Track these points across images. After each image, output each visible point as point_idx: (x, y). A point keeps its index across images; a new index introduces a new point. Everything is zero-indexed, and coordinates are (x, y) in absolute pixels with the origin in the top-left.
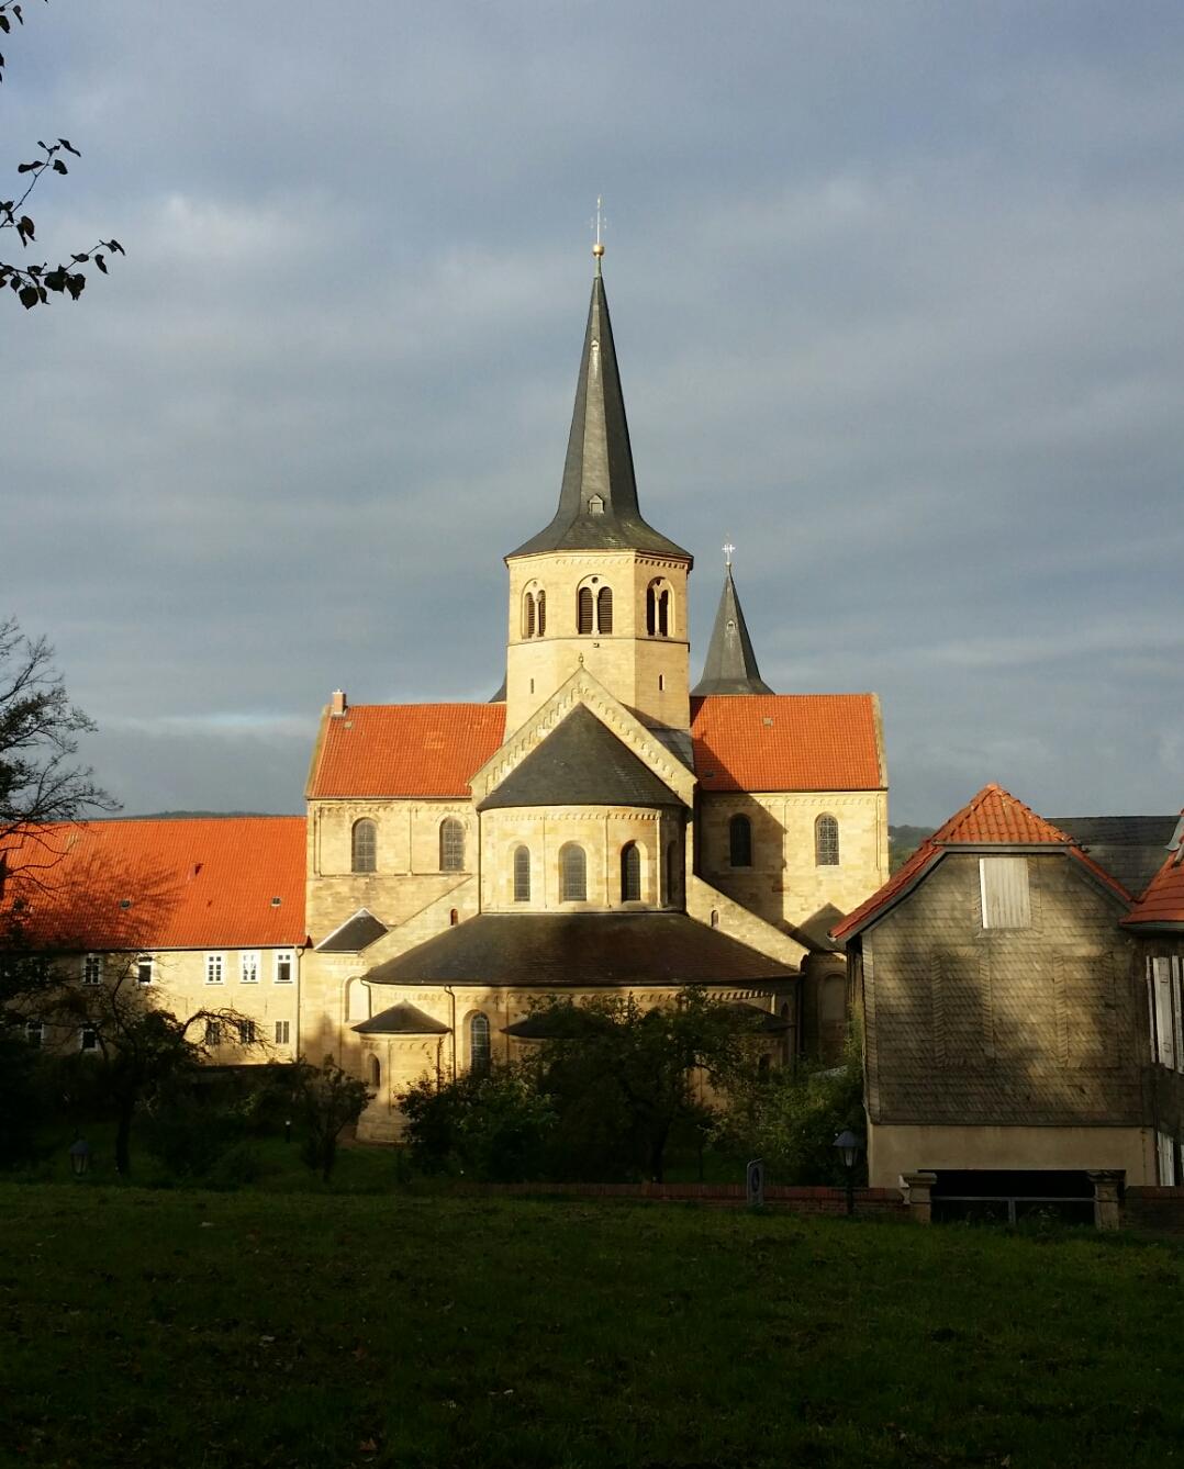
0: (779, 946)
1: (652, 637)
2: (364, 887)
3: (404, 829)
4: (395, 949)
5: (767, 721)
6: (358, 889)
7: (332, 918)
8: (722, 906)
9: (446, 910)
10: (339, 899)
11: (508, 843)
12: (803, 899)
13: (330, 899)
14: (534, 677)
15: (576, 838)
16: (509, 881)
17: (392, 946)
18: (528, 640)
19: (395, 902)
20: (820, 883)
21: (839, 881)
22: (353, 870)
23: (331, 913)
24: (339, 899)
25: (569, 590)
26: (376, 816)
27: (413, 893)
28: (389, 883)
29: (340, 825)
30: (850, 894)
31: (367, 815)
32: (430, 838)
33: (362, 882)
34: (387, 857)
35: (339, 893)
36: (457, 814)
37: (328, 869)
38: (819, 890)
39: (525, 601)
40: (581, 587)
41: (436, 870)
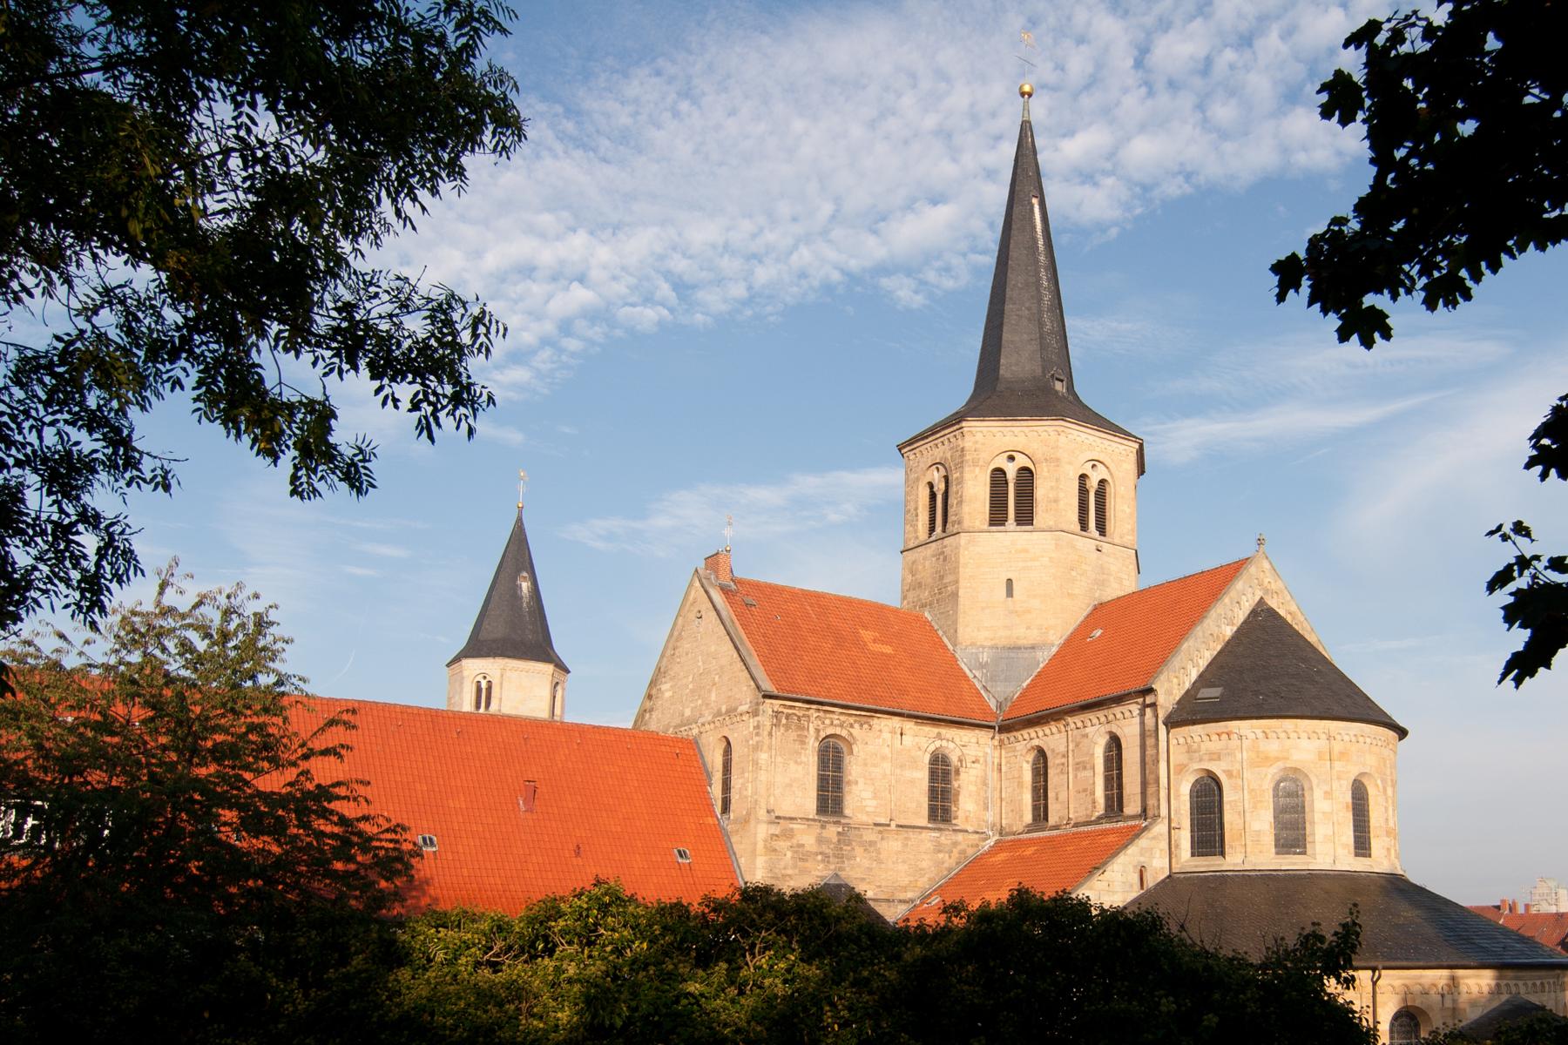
2: (835, 840)
3: (884, 758)
6: (828, 841)
9: (1135, 867)
10: (801, 855)
13: (789, 854)
28: (870, 836)
29: (803, 743)
31: (838, 731)
33: (832, 831)
34: (860, 799)
35: (803, 845)
36: (951, 745)
37: (786, 807)
41: (924, 822)
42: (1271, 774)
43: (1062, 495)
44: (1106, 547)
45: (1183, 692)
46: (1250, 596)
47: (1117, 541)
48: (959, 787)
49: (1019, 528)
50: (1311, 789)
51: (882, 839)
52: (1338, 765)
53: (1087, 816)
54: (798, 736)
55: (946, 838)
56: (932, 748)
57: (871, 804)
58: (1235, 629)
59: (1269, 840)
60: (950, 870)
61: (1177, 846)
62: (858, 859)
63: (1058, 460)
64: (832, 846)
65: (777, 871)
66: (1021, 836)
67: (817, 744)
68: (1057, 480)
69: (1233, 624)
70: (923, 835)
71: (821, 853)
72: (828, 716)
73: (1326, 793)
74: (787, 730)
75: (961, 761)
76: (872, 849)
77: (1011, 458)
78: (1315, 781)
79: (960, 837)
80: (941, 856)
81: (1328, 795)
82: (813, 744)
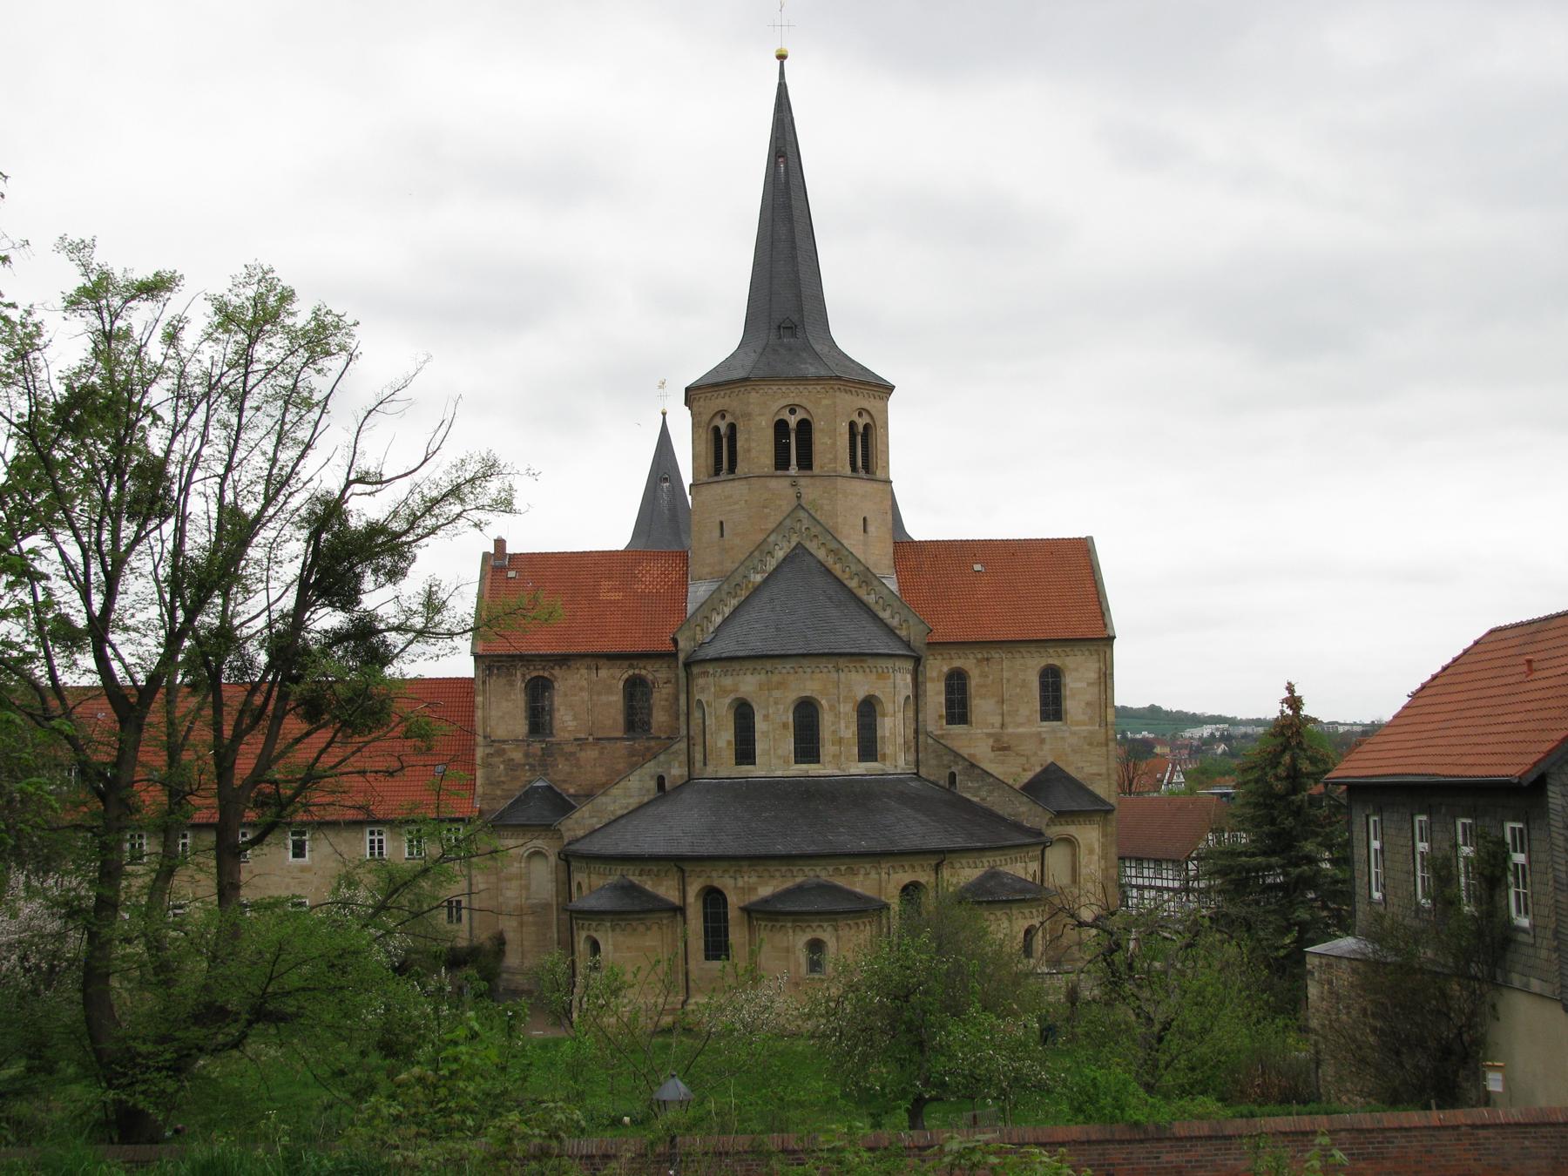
0: (1023, 809)
1: (855, 475)
2: (540, 753)
4: (595, 820)
5: (977, 567)
7: (505, 787)
8: (960, 767)
9: (652, 777)
10: (512, 766)
11: (728, 701)
12: (1025, 759)
13: (502, 767)
15: (808, 694)
16: (729, 742)
17: (591, 817)
18: (716, 479)
19: (575, 770)
20: (1042, 741)
21: (1063, 738)
23: (503, 782)
24: (512, 766)
25: (764, 423)
26: (552, 675)
27: (595, 759)
28: (568, 748)
30: (1074, 751)
31: (541, 673)
32: (614, 698)
33: (537, 747)
34: (566, 719)
35: (513, 760)
37: (500, 732)
38: (1042, 750)
39: (711, 436)
40: (777, 418)
43: (753, 445)
44: (803, 482)
52: (777, 694)
67: (523, 685)
69: (764, 571)
70: (618, 745)
73: (764, 716)
75: (654, 684)
78: (755, 708)
79: (653, 743)
80: (634, 759)
81: (766, 717)
82: (520, 685)
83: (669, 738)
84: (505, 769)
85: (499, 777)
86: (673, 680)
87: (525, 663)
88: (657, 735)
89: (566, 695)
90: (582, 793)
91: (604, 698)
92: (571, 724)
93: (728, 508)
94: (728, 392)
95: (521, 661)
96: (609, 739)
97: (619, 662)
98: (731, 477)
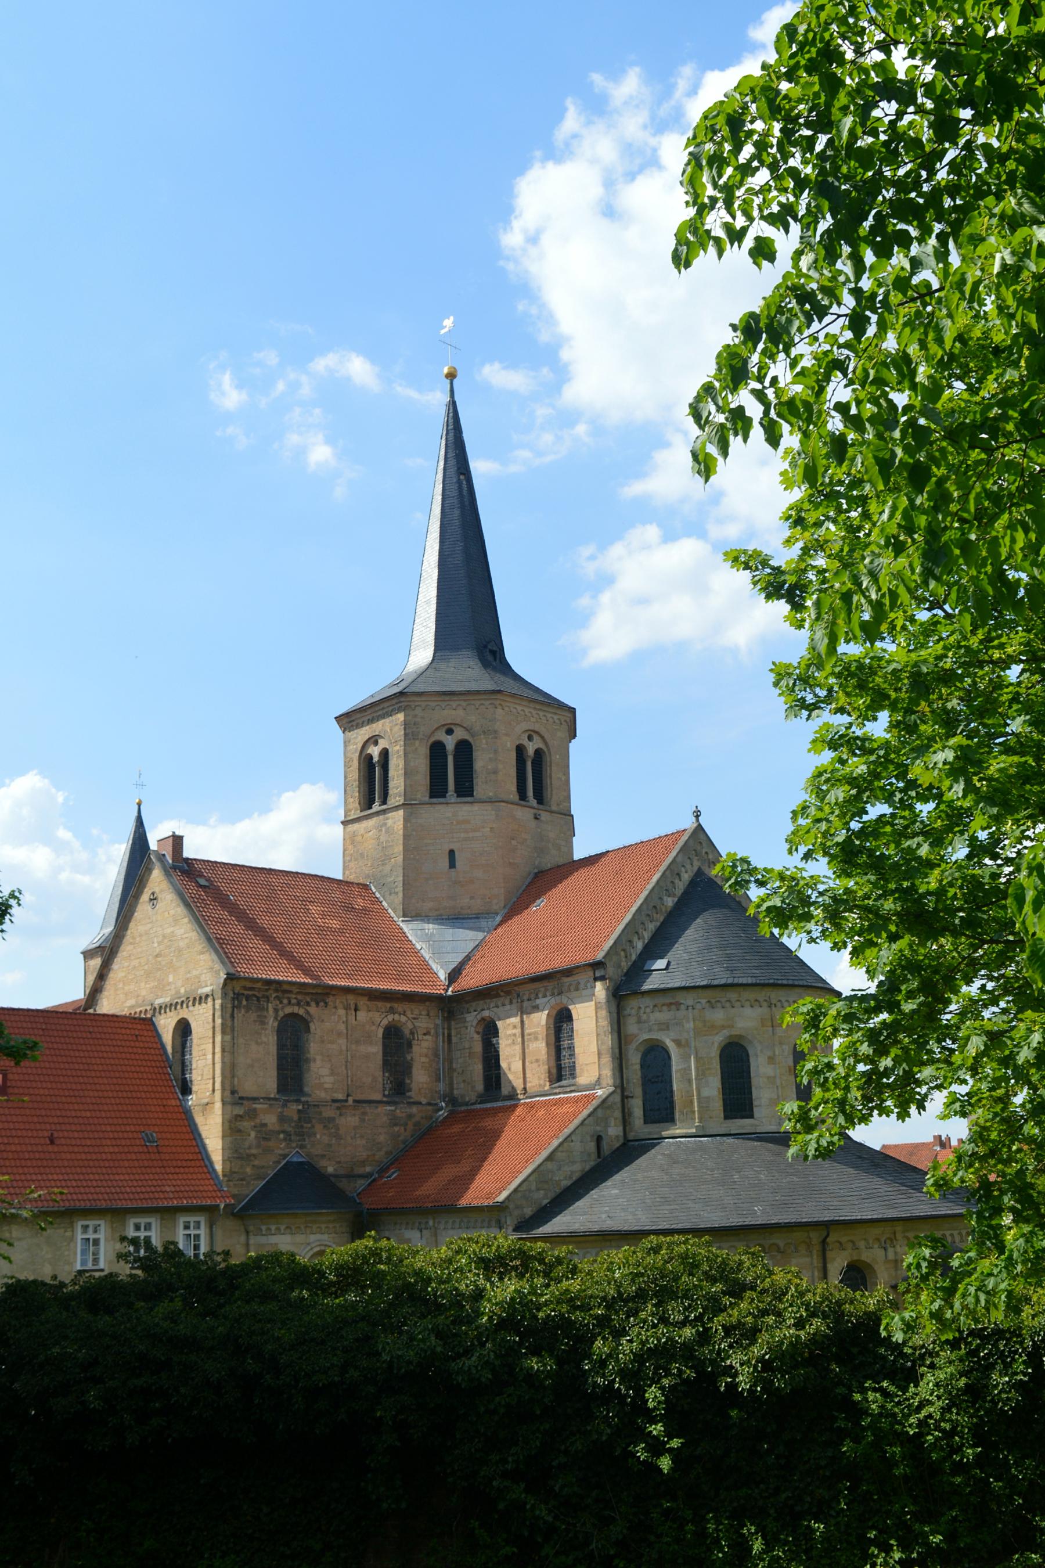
2: (296, 1117)
3: (339, 1034)
7: (256, 1163)
9: (592, 1136)
10: (265, 1134)
13: (253, 1134)
14: (452, 846)
17: (538, 1189)
22: (279, 1092)
24: (265, 1134)
26: (308, 1012)
27: (355, 1128)
28: (328, 1112)
29: (263, 1023)
31: (296, 1010)
35: (265, 1125)
36: (403, 1019)
37: (249, 1087)
42: (718, 1039)
43: (500, 766)
44: (544, 816)
45: (630, 964)
46: (688, 867)
47: (554, 808)
48: (412, 1059)
49: (459, 800)
50: (757, 1056)
51: (341, 1115)
53: (540, 1085)
54: (258, 1016)
55: (400, 1112)
56: (385, 1022)
57: (328, 1081)
58: (676, 899)
59: (717, 1105)
60: (404, 1142)
61: (630, 1114)
62: (318, 1136)
63: (496, 732)
64: (293, 1124)
65: (242, 1151)
66: (473, 1107)
67: (276, 1024)
68: (496, 752)
69: (674, 895)
70: (379, 1109)
71: (283, 1132)
72: (286, 995)
73: (769, 1058)
74: (247, 1012)
75: (412, 1033)
76: (331, 1125)
77: (450, 732)
79: (414, 1109)
80: (396, 1129)
81: (771, 1060)
82: (272, 1023)
83: (429, 1104)
84: (256, 1137)
85: (250, 1148)
86: (432, 1031)
87: (280, 994)
88: (416, 1099)
89: (323, 1042)
90: (342, 1172)
91: (364, 1049)
92: (328, 1081)
93: (463, 835)
94: (464, 704)
95: (276, 991)
96: (370, 1102)
97: (380, 1004)
98: (384, 807)
